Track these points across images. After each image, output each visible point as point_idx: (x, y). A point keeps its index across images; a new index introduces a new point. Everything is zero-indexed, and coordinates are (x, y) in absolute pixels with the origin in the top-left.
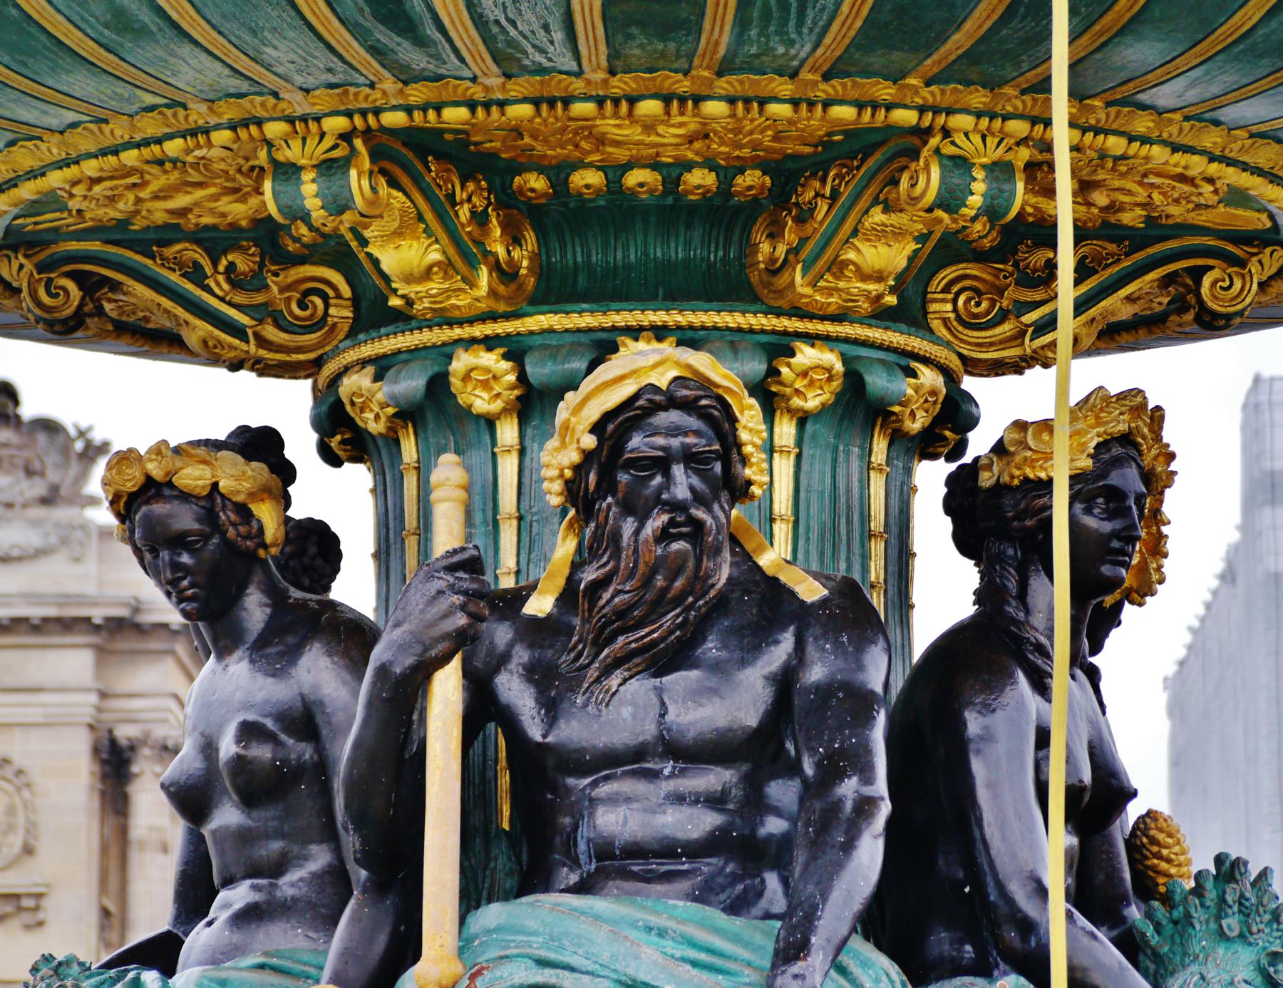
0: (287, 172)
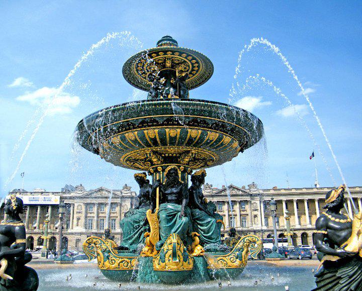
0: (147, 154)
